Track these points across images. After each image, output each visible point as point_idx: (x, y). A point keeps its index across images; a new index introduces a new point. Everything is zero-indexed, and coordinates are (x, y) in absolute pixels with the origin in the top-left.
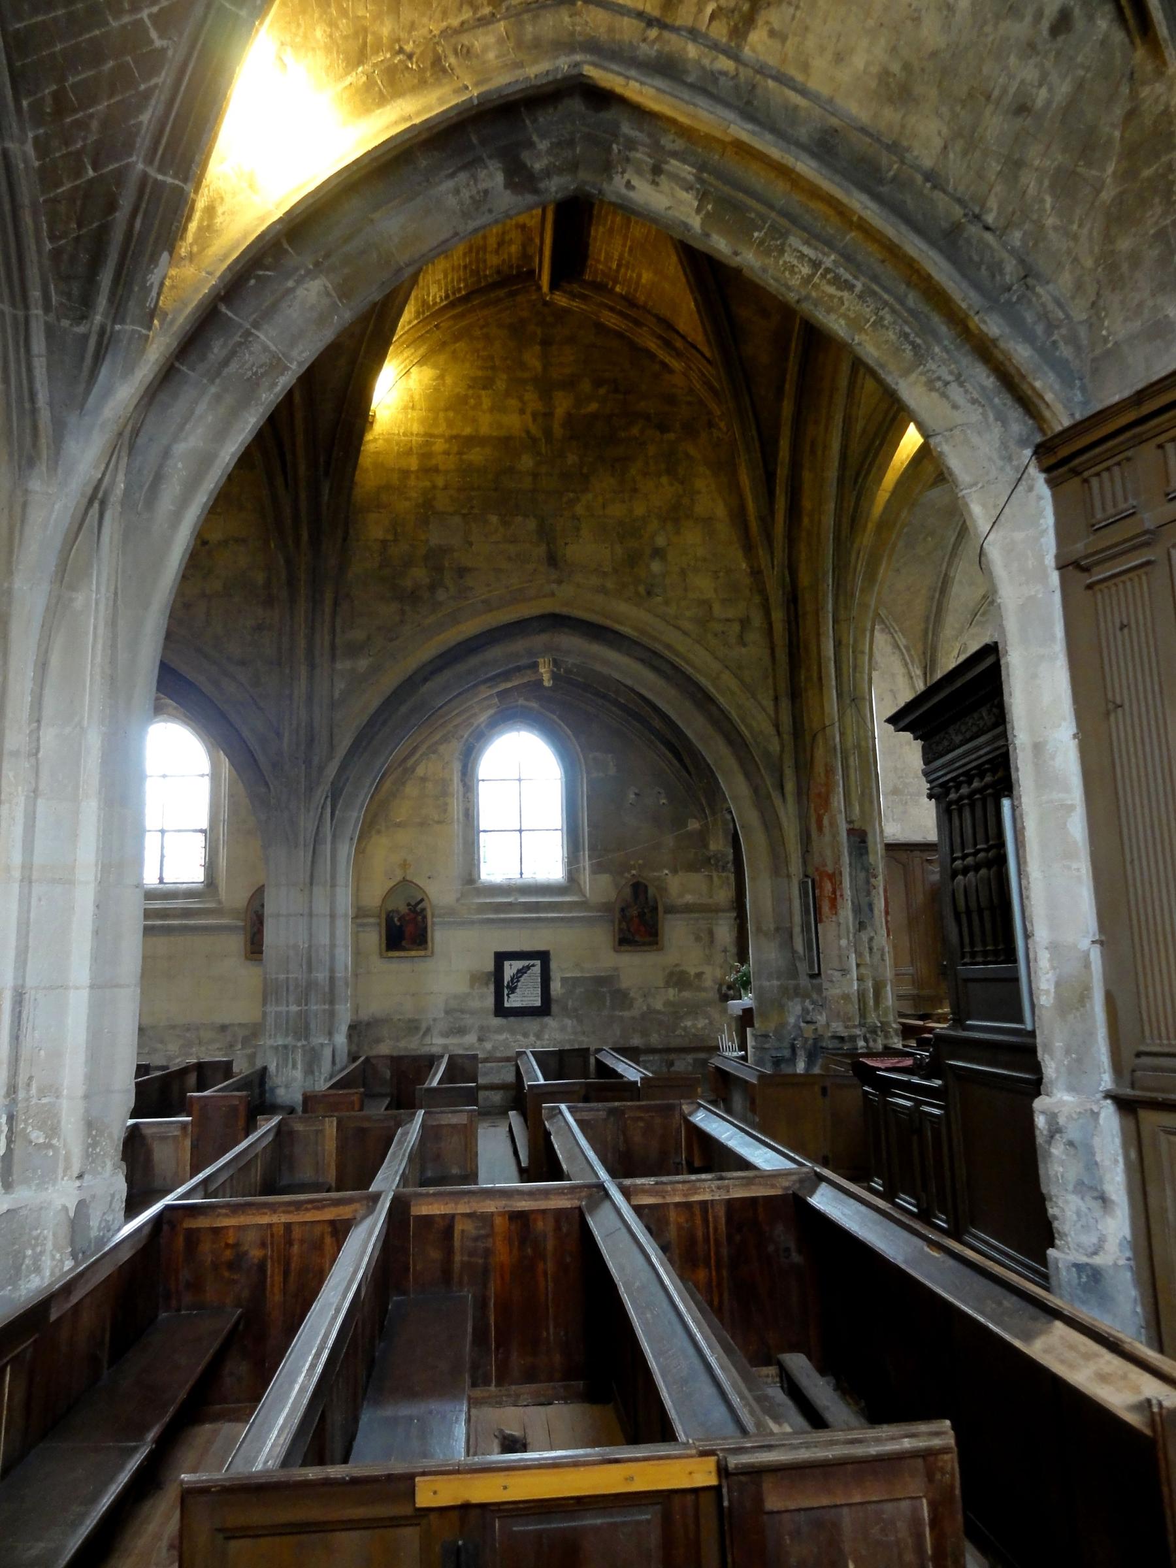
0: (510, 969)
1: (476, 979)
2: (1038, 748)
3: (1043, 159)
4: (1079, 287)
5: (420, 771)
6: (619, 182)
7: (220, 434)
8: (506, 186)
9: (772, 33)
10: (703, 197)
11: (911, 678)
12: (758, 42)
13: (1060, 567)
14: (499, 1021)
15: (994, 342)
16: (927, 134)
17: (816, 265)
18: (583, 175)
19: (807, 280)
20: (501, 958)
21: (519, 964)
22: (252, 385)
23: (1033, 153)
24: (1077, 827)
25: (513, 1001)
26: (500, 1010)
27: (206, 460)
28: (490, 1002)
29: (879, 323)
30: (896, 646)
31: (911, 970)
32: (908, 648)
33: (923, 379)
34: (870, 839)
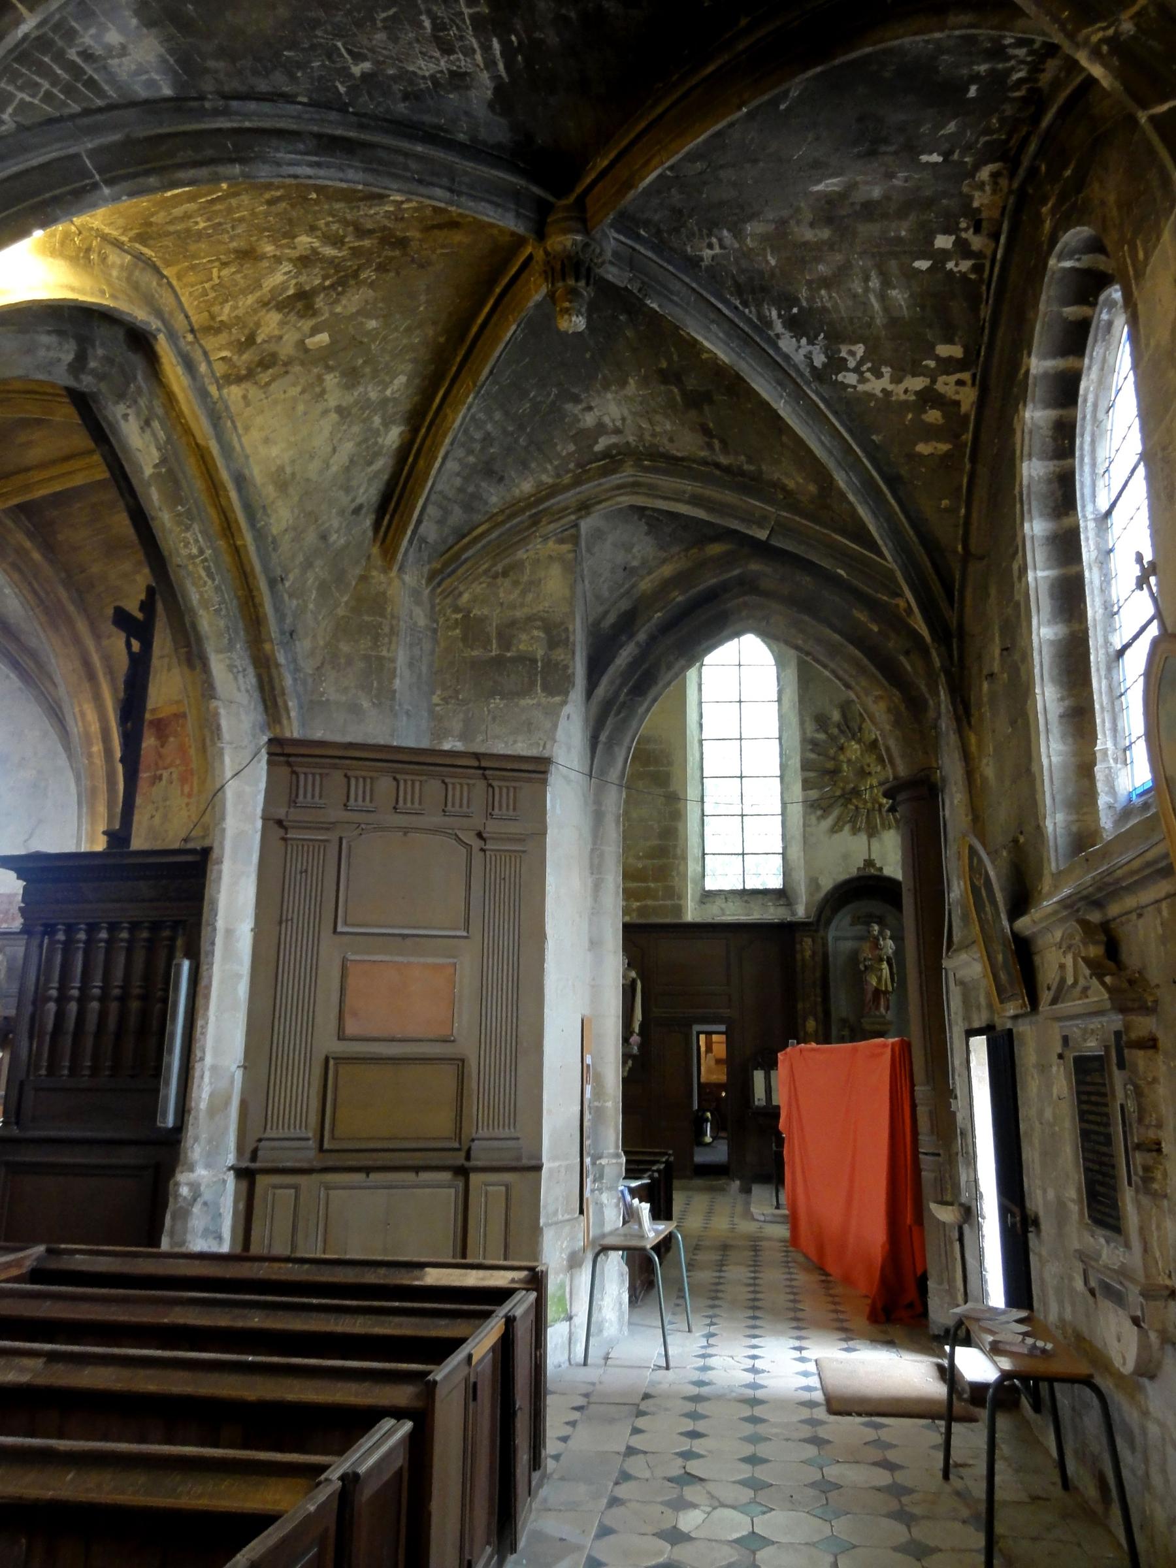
2: (229, 932)
3: (320, 570)
4: (312, 653)
6: (120, 409)
8: (69, 364)
9: (245, 397)
10: (164, 461)
12: (234, 393)
13: (265, 819)
15: (278, 665)
16: (281, 516)
17: (201, 552)
18: (103, 386)
19: (192, 557)
23: (319, 563)
24: (243, 989)
29: (218, 611)
33: (228, 662)
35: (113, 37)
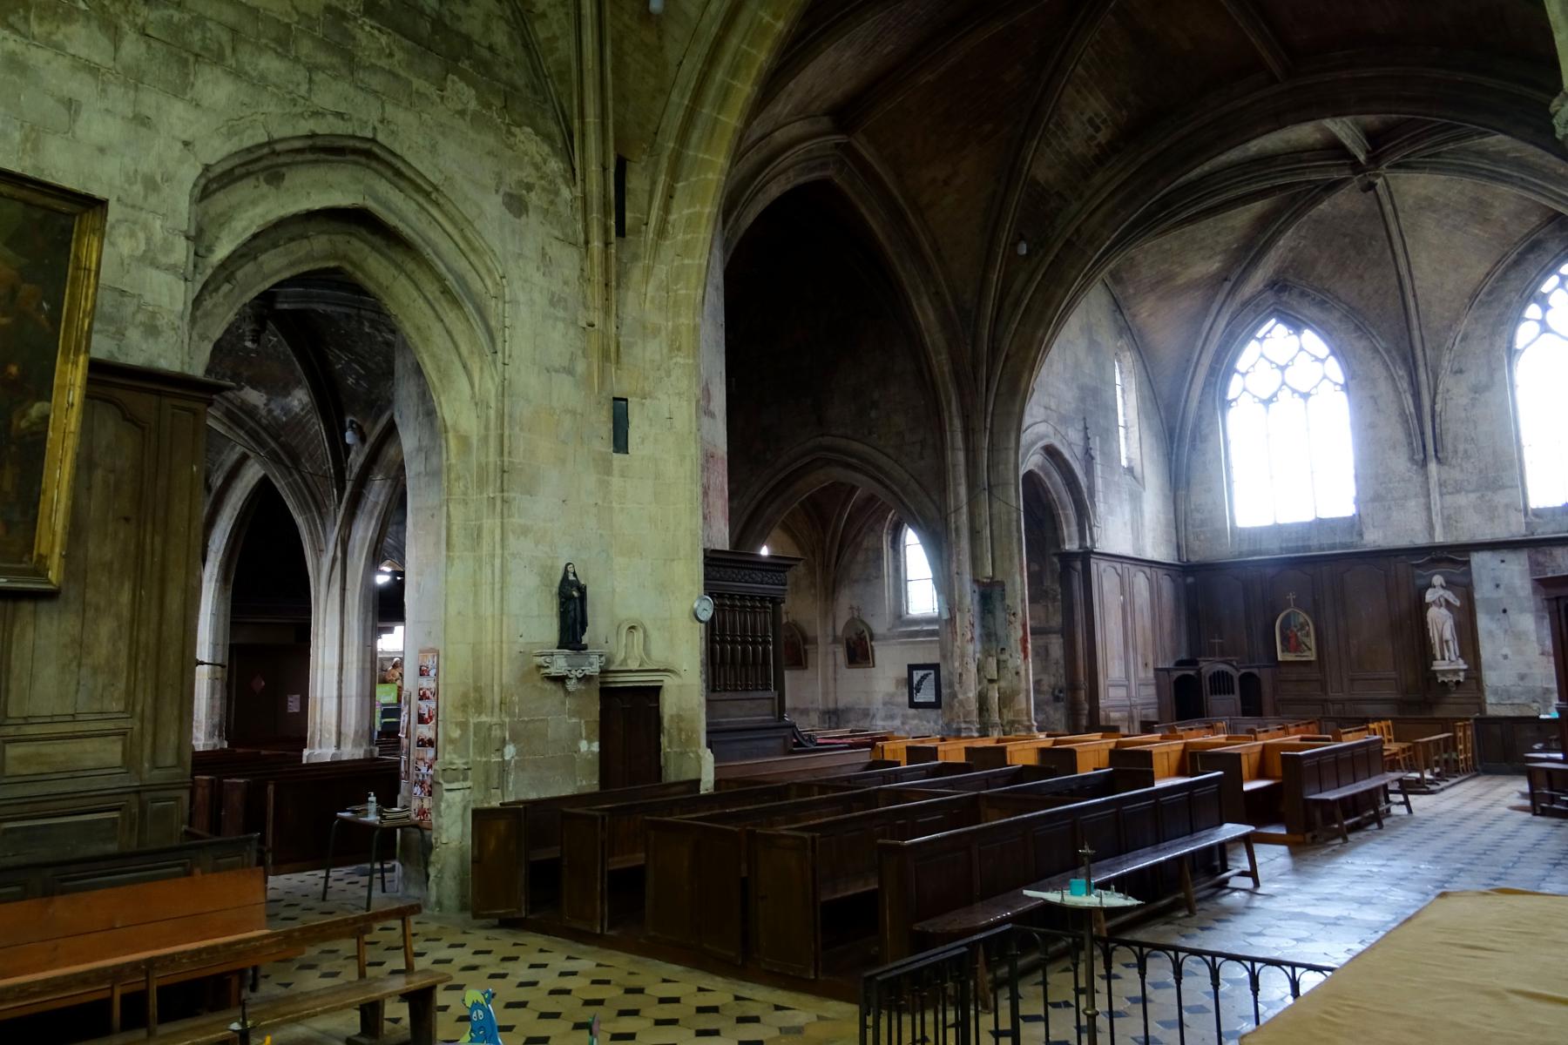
0: (917, 675)
1: (898, 682)
5: (865, 544)
7: (367, 530)
11: (1394, 380)
14: (913, 711)
20: (912, 668)
21: (921, 673)
22: (372, 513)
25: (919, 698)
26: (913, 705)
27: (364, 539)
28: (906, 699)
30: (1376, 351)
31: (1393, 674)
32: (1388, 351)
34: (1008, 588)
35: (296, 403)
